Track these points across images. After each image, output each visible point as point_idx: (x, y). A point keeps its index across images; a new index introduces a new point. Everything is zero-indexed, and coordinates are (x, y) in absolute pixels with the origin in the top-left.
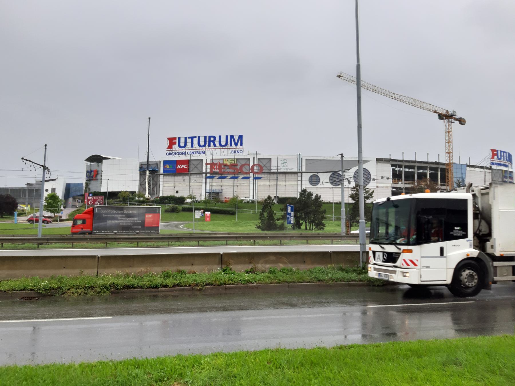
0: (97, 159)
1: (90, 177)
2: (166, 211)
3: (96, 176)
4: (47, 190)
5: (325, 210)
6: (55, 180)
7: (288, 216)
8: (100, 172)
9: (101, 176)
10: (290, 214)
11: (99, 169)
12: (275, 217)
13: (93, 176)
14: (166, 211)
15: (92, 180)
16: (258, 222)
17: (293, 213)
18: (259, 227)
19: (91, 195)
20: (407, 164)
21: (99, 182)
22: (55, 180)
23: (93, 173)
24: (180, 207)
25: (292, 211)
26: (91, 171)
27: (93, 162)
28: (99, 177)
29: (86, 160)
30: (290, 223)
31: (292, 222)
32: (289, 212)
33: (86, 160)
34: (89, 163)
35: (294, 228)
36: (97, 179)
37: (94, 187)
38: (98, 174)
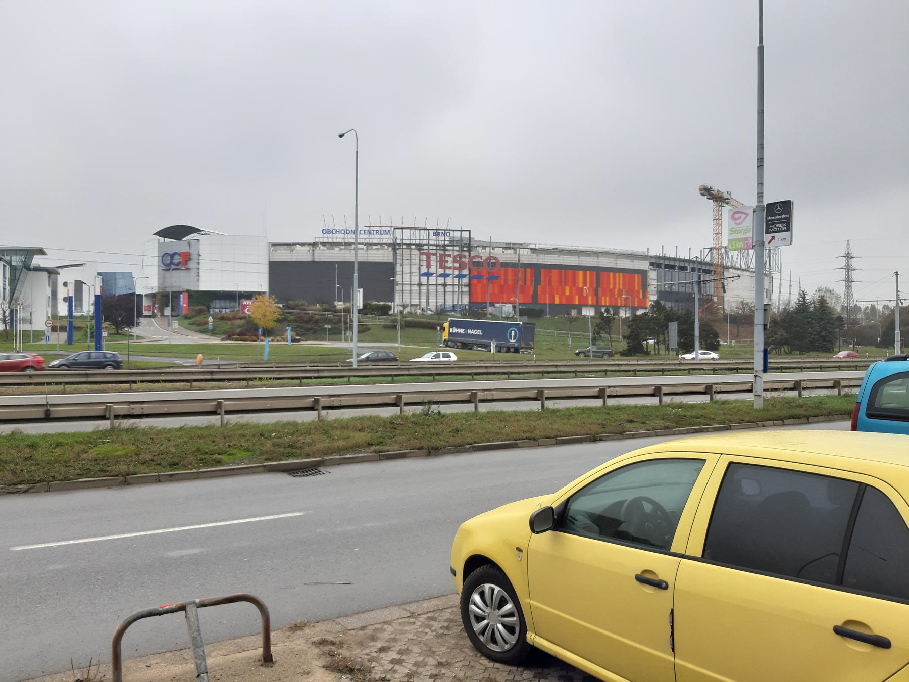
0: (177, 232)
1: (171, 263)
6: (81, 265)
8: (194, 256)
9: (199, 263)
11: (193, 251)
13: (174, 262)
20: (667, 262)
21: (193, 273)
22: (81, 265)
23: (177, 256)
26: (172, 256)
28: (192, 265)
29: (155, 234)
33: (155, 234)
36: (188, 269)
37: (181, 281)
38: (190, 259)
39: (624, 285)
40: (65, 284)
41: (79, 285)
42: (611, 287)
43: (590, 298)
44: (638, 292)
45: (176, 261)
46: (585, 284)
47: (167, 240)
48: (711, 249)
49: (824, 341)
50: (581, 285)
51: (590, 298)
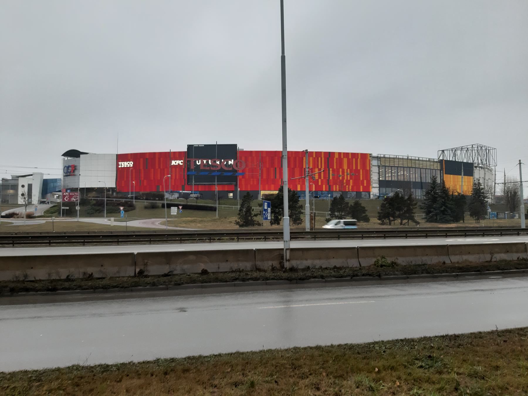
0: (74, 154)
2: (146, 208)
3: (74, 172)
4: (23, 186)
5: (302, 206)
6: (32, 175)
7: (264, 212)
8: (78, 168)
10: (267, 210)
12: (253, 213)
13: (70, 171)
14: (146, 208)
15: (70, 175)
16: (235, 218)
17: (269, 210)
18: (237, 223)
19: (68, 191)
22: (32, 175)
23: (70, 168)
24: (159, 203)
25: (268, 207)
27: (70, 156)
28: (76, 172)
29: (63, 155)
30: (266, 218)
31: (269, 218)
32: (266, 208)
33: (63, 155)
34: (66, 158)
35: (272, 223)
36: (74, 175)
37: (71, 183)
38: (75, 169)
39: (351, 179)
40: (23, 186)
41: (30, 186)
42: (341, 178)
43: (324, 186)
44: (363, 181)
45: (70, 171)
46: (320, 177)
47: (69, 158)
48: (443, 151)
49: (444, 214)
50: (317, 177)
51: (324, 186)
